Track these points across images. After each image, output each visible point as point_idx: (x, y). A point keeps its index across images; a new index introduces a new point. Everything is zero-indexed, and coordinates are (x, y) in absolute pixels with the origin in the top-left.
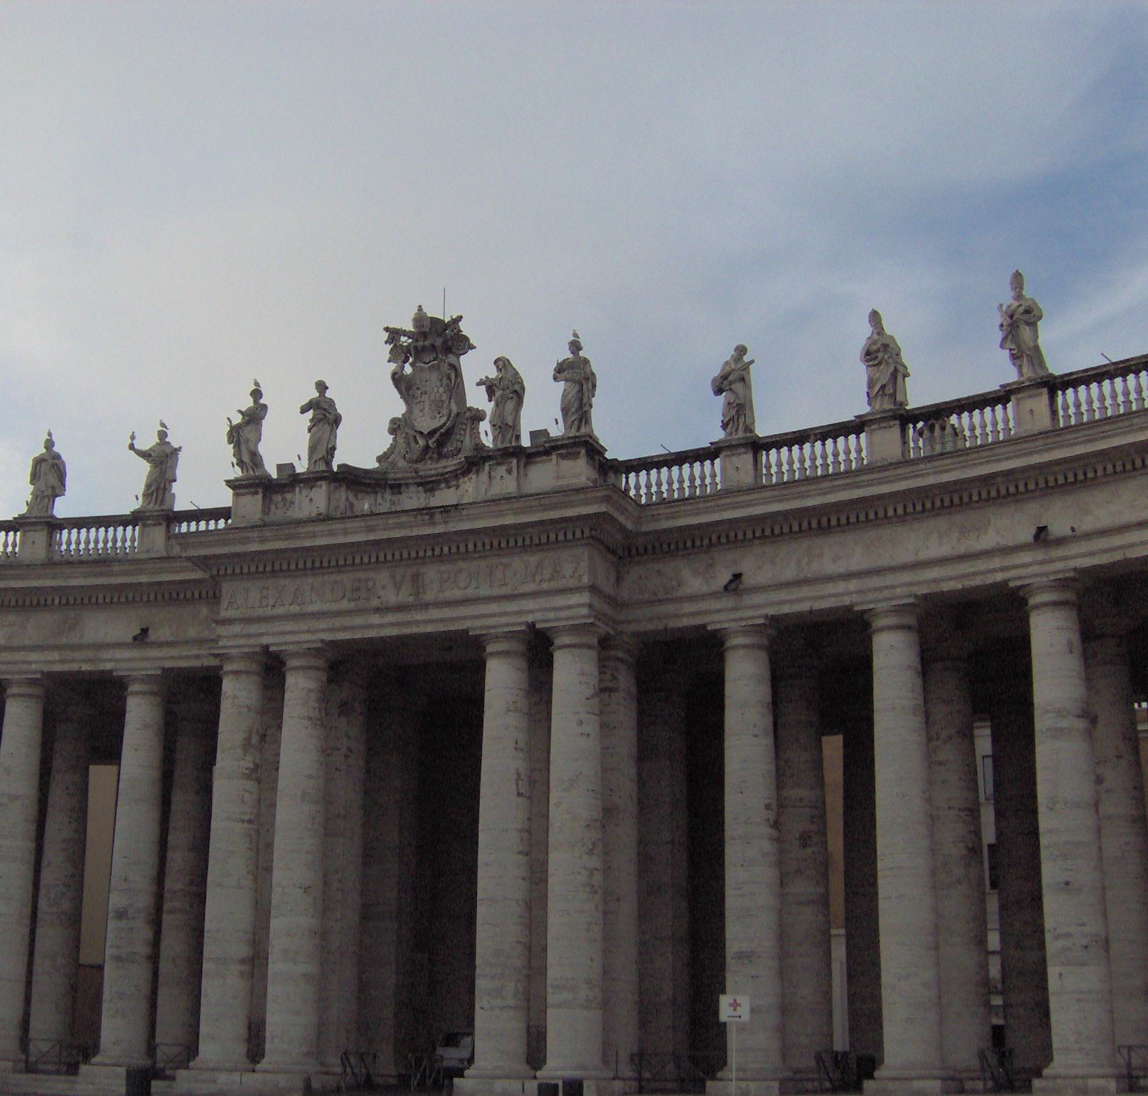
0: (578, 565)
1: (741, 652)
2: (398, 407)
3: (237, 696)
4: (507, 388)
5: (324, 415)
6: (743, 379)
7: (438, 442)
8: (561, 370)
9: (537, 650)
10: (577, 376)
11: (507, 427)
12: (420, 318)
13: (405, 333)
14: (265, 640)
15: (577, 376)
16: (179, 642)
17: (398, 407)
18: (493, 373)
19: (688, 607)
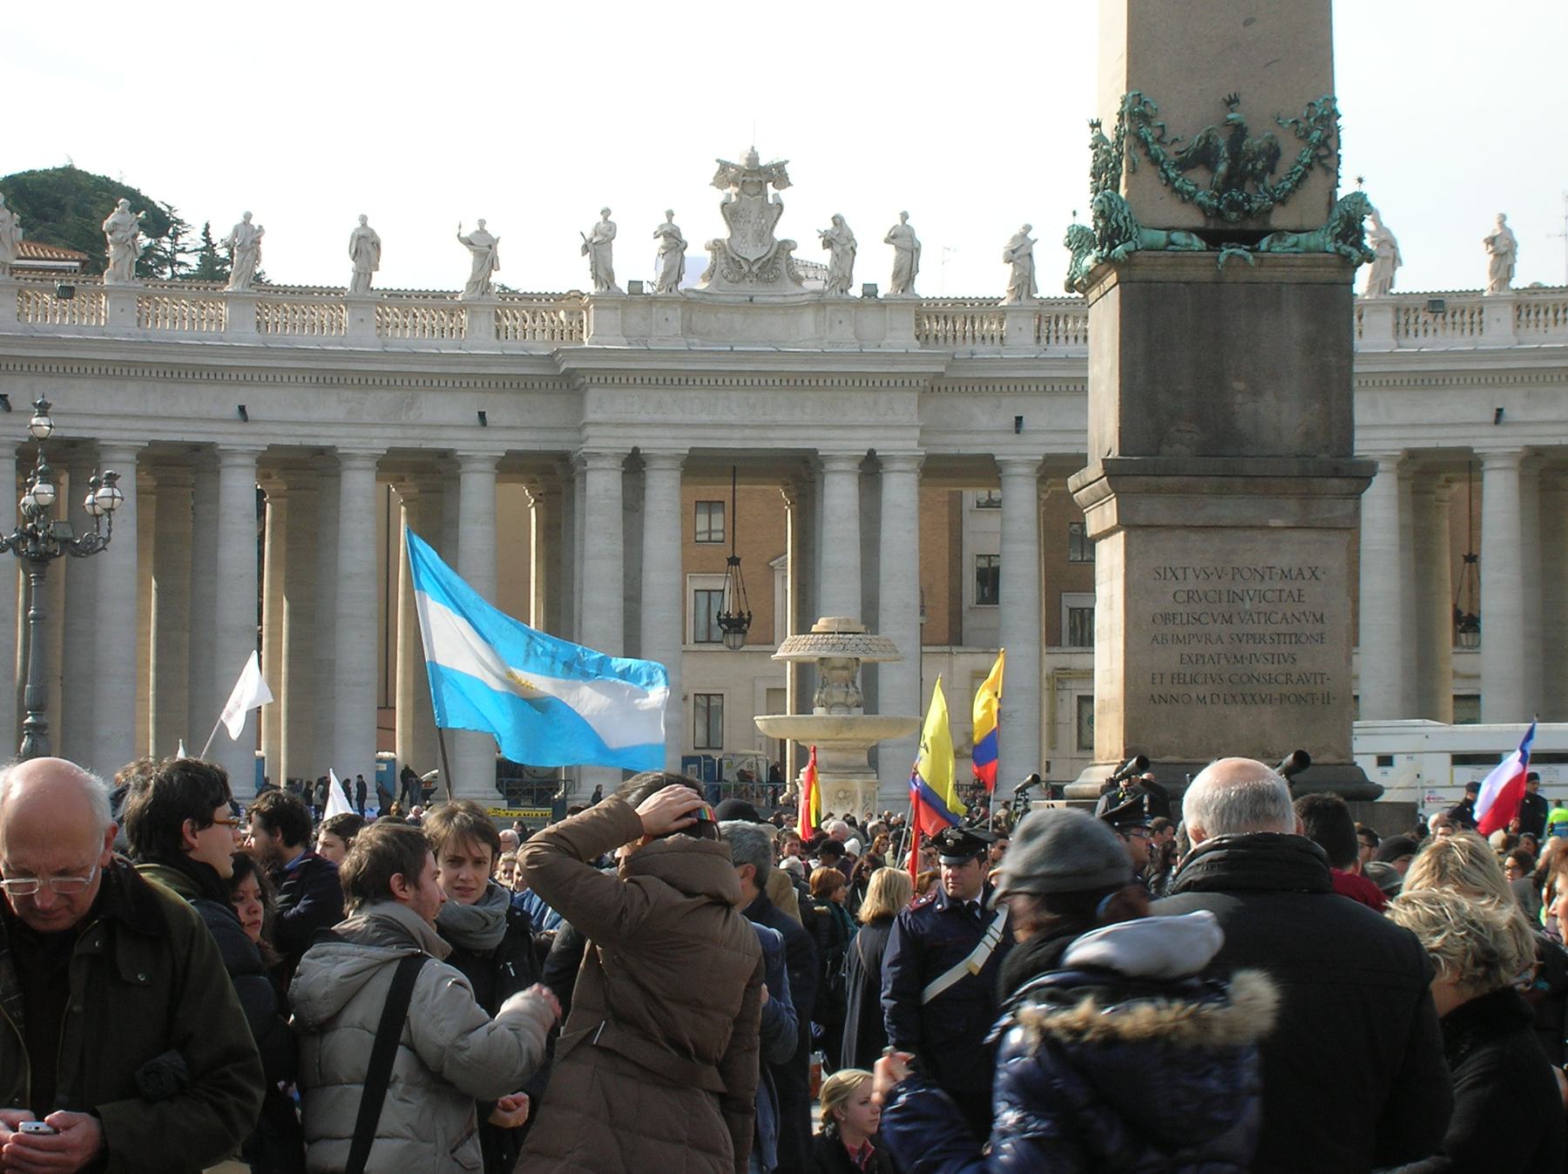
0: (905, 408)
1: (1020, 480)
2: (722, 232)
3: (601, 487)
4: (839, 240)
5: (673, 242)
6: (1030, 255)
7: (753, 263)
8: (891, 239)
9: (871, 468)
10: (906, 245)
11: (841, 275)
12: (753, 158)
13: (733, 166)
14: (640, 444)
15: (906, 245)
16: (523, 427)
17: (722, 232)
18: (829, 225)
19: (981, 439)
